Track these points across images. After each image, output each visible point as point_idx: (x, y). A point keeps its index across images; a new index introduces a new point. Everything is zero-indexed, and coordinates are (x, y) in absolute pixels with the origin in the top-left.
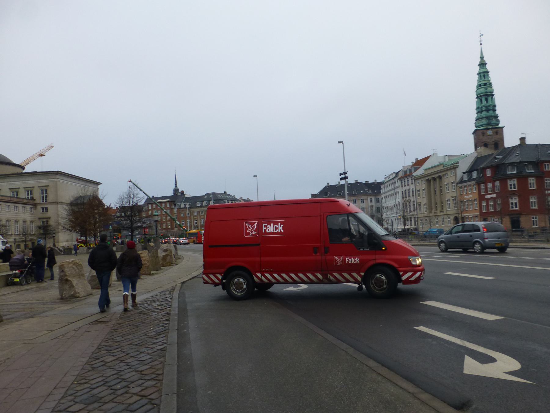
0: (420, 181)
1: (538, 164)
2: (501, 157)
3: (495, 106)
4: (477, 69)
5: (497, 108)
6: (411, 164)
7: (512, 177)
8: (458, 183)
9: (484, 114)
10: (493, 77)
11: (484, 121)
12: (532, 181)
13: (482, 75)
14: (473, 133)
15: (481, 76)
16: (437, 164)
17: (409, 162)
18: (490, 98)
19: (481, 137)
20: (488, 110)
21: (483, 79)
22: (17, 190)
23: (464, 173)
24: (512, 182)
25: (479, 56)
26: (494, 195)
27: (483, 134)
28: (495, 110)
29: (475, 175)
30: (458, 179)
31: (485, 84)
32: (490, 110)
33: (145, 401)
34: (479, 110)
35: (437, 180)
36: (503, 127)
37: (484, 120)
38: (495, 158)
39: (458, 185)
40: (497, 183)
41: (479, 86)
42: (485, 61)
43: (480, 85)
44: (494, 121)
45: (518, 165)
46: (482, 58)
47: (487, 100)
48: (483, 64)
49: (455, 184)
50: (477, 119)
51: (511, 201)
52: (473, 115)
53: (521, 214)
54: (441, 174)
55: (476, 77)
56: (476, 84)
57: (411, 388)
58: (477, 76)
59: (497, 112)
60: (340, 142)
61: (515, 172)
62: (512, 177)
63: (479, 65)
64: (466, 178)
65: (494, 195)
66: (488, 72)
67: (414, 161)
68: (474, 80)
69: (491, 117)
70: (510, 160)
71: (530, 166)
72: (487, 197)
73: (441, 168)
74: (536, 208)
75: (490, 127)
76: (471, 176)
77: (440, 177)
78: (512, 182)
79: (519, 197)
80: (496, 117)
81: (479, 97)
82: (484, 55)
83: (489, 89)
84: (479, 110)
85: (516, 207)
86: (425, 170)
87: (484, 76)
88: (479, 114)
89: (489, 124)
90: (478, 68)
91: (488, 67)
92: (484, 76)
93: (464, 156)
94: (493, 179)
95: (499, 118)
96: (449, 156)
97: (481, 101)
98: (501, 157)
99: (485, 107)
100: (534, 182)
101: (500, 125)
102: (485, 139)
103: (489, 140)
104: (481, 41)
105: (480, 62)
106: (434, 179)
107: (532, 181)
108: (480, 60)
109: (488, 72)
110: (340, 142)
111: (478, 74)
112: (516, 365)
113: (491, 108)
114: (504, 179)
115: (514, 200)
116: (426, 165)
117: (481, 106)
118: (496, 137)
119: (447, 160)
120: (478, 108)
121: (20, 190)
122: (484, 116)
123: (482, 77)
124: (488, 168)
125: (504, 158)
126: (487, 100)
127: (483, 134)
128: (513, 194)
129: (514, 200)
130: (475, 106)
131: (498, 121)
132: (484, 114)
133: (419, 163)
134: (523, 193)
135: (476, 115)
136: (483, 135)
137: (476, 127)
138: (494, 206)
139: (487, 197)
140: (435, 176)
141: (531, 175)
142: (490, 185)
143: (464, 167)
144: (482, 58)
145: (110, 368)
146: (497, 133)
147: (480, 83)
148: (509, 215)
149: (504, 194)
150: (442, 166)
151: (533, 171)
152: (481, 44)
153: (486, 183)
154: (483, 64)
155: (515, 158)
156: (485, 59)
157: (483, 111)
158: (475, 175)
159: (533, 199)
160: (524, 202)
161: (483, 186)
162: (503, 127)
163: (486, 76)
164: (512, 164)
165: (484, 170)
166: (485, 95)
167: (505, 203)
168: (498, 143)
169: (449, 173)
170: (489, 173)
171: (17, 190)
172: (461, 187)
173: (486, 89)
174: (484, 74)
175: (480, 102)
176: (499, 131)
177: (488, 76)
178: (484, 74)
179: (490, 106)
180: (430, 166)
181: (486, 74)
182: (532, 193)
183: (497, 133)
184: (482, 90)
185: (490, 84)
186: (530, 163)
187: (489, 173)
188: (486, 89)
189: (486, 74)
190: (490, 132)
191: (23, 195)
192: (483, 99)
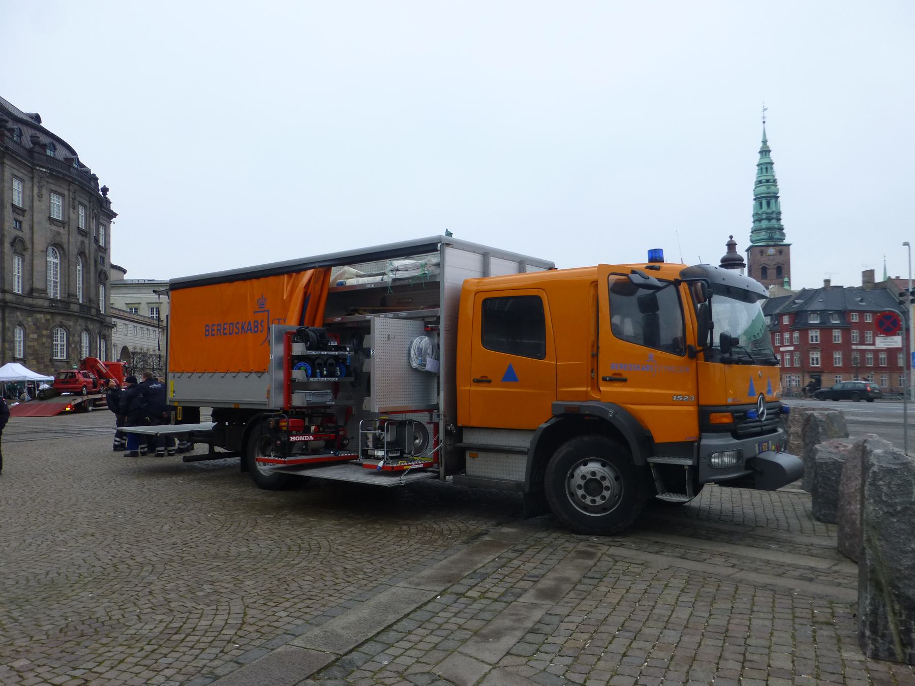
1: (844, 314)
3: (780, 213)
4: (757, 158)
5: (782, 216)
7: (814, 327)
9: (764, 224)
10: (779, 172)
11: (764, 235)
12: (837, 333)
13: (764, 167)
14: (747, 251)
15: (762, 169)
18: (773, 201)
19: (759, 256)
20: (769, 219)
21: (764, 173)
22: (136, 306)
24: (814, 334)
25: (761, 139)
26: (792, 348)
27: (762, 252)
28: (779, 220)
31: (768, 181)
34: (756, 218)
38: (795, 303)
40: (796, 334)
44: (777, 236)
45: (823, 313)
46: (765, 142)
47: (768, 204)
48: (765, 152)
50: (754, 231)
51: (811, 356)
53: (823, 372)
55: (755, 170)
59: (782, 222)
61: (818, 322)
62: (814, 327)
65: (792, 348)
66: (773, 164)
68: (752, 174)
69: (774, 228)
70: (812, 307)
71: (836, 316)
72: (782, 349)
78: (814, 334)
79: (822, 351)
80: (781, 229)
81: (758, 199)
82: (768, 138)
83: (773, 187)
84: (758, 218)
87: (767, 168)
88: (757, 224)
89: (771, 238)
90: (759, 156)
91: (773, 156)
92: (767, 168)
94: (791, 329)
97: (761, 204)
99: (766, 213)
101: (786, 242)
102: (763, 260)
103: (769, 263)
104: (764, 118)
105: (762, 148)
107: (837, 333)
108: (761, 145)
109: (773, 164)
113: (774, 216)
114: (805, 330)
115: (816, 355)
117: (760, 212)
118: (780, 259)
120: (755, 215)
121: (141, 306)
122: (764, 227)
123: (764, 170)
125: (806, 303)
126: (768, 204)
127: (762, 252)
128: (814, 347)
129: (816, 355)
130: (751, 212)
131: (784, 235)
132: (764, 224)
134: (827, 348)
135: (752, 225)
137: (752, 241)
138: (792, 360)
139: (782, 349)
141: (836, 327)
142: (787, 335)
144: (765, 142)
146: (781, 252)
148: (809, 372)
149: (804, 348)
151: (838, 322)
153: (781, 332)
154: (765, 152)
155: (818, 305)
156: (768, 144)
157: (762, 219)
159: (837, 355)
160: (827, 358)
161: (777, 337)
164: (814, 312)
165: (780, 316)
167: (805, 359)
170: (786, 320)
171: (136, 306)
173: (769, 188)
174: (766, 167)
176: (784, 250)
177: (772, 168)
178: (766, 167)
179: (773, 213)
181: (769, 166)
182: (837, 347)
183: (781, 252)
184: (763, 189)
185: (775, 181)
186: (837, 312)
187: (786, 320)
188: (769, 188)
189: (769, 166)
190: (771, 251)
191: (145, 312)
192: (764, 202)
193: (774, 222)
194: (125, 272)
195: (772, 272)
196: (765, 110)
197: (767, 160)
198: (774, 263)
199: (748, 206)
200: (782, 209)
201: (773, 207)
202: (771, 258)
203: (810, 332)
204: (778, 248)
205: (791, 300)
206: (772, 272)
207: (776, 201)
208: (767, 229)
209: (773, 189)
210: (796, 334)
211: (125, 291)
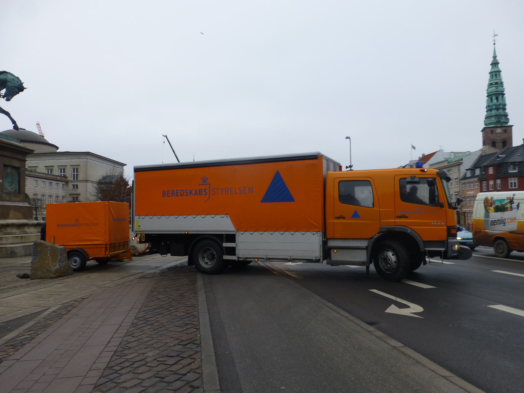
2: (504, 156)
3: (505, 105)
4: (489, 68)
5: (507, 107)
6: (418, 159)
7: (513, 175)
9: (494, 112)
10: (505, 77)
11: (493, 120)
13: (494, 74)
14: (482, 131)
15: (492, 75)
16: (443, 159)
17: (416, 156)
18: (500, 97)
20: (497, 109)
22: (51, 168)
23: (467, 170)
25: (492, 55)
27: (492, 132)
28: (504, 109)
29: (478, 172)
30: (462, 175)
31: (497, 83)
33: (188, 315)
34: (488, 108)
36: (512, 126)
37: (493, 119)
38: (498, 157)
39: (461, 181)
40: (499, 181)
41: (491, 85)
42: (497, 60)
43: (491, 84)
44: (503, 120)
46: (495, 57)
47: (497, 99)
48: (495, 64)
50: (486, 118)
52: (483, 113)
55: (488, 76)
56: (487, 83)
57: (346, 314)
58: (489, 75)
59: (507, 111)
60: (347, 138)
61: (516, 171)
62: (513, 175)
63: (491, 64)
64: (469, 174)
66: (500, 72)
67: (421, 156)
68: (486, 79)
69: (501, 115)
73: (446, 164)
75: (499, 125)
76: (474, 173)
80: (506, 115)
81: (490, 96)
82: (497, 54)
83: (500, 87)
84: (489, 109)
86: (431, 165)
87: (496, 75)
89: (498, 122)
90: (490, 67)
91: (501, 67)
92: (496, 75)
93: (469, 154)
94: (494, 177)
95: (508, 117)
96: (455, 153)
97: (492, 99)
98: (504, 156)
99: (495, 105)
101: (509, 124)
102: (493, 137)
103: (497, 138)
104: (494, 41)
108: (492, 59)
109: (500, 72)
110: (347, 138)
111: (490, 73)
112: (420, 309)
113: (501, 106)
116: (432, 161)
117: (491, 104)
118: (505, 136)
119: (452, 157)
120: (488, 106)
121: (54, 168)
122: (493, 114)
123: (494, 76)
124: (490, 166)
127: (492, 132)
130: (485, 105)
131: (508, 119)
132: (494, 112)
133: (426, 158)
135: (486, 113)
137: (485, 125)
142: (491, 183)
143: (468, 164)
144: (495, 57)
145: (163, 301)
146: (505, 131)
150: (447, 162)
152: (494, 44)
153: (487, 180)
154: (495, 64)
155: (517, 158)
156: (497, 58)
162: (512, 126)
163: (498, 76)
164: (514, 164)
165: (486, 168)
166: (496, 95)
168: (507, 141)
169: (453, 169)
170: (491, 171)
171: (51, 168)
172: (464, 184)
173: (497, 88)
174: (495, 73)
175: (490, 101)
176: (508, 130)
177: (500, 75)
178: (495, 73)
179: (500, 105)
180: (436, 162)
181: (497, 73)
183: (505, 131)
184: (493, 89)
185: (502, 83)
187: (491, 171)
188: (497, 88)
189: (497, 73)
190: (499, 130)
191: (56, 172)
192: (494, 98)
193: (501, 111)
194: (57, 148)
196: (495, 35)
197: (496, 69)
198: (501, 138)
201: (500, 101)
202: (498, 135)
203: (509, 179)
205: (496, 155)
208: (496, 116)
209: (500, 89)
210: (499, 181)
211: (44, 158)
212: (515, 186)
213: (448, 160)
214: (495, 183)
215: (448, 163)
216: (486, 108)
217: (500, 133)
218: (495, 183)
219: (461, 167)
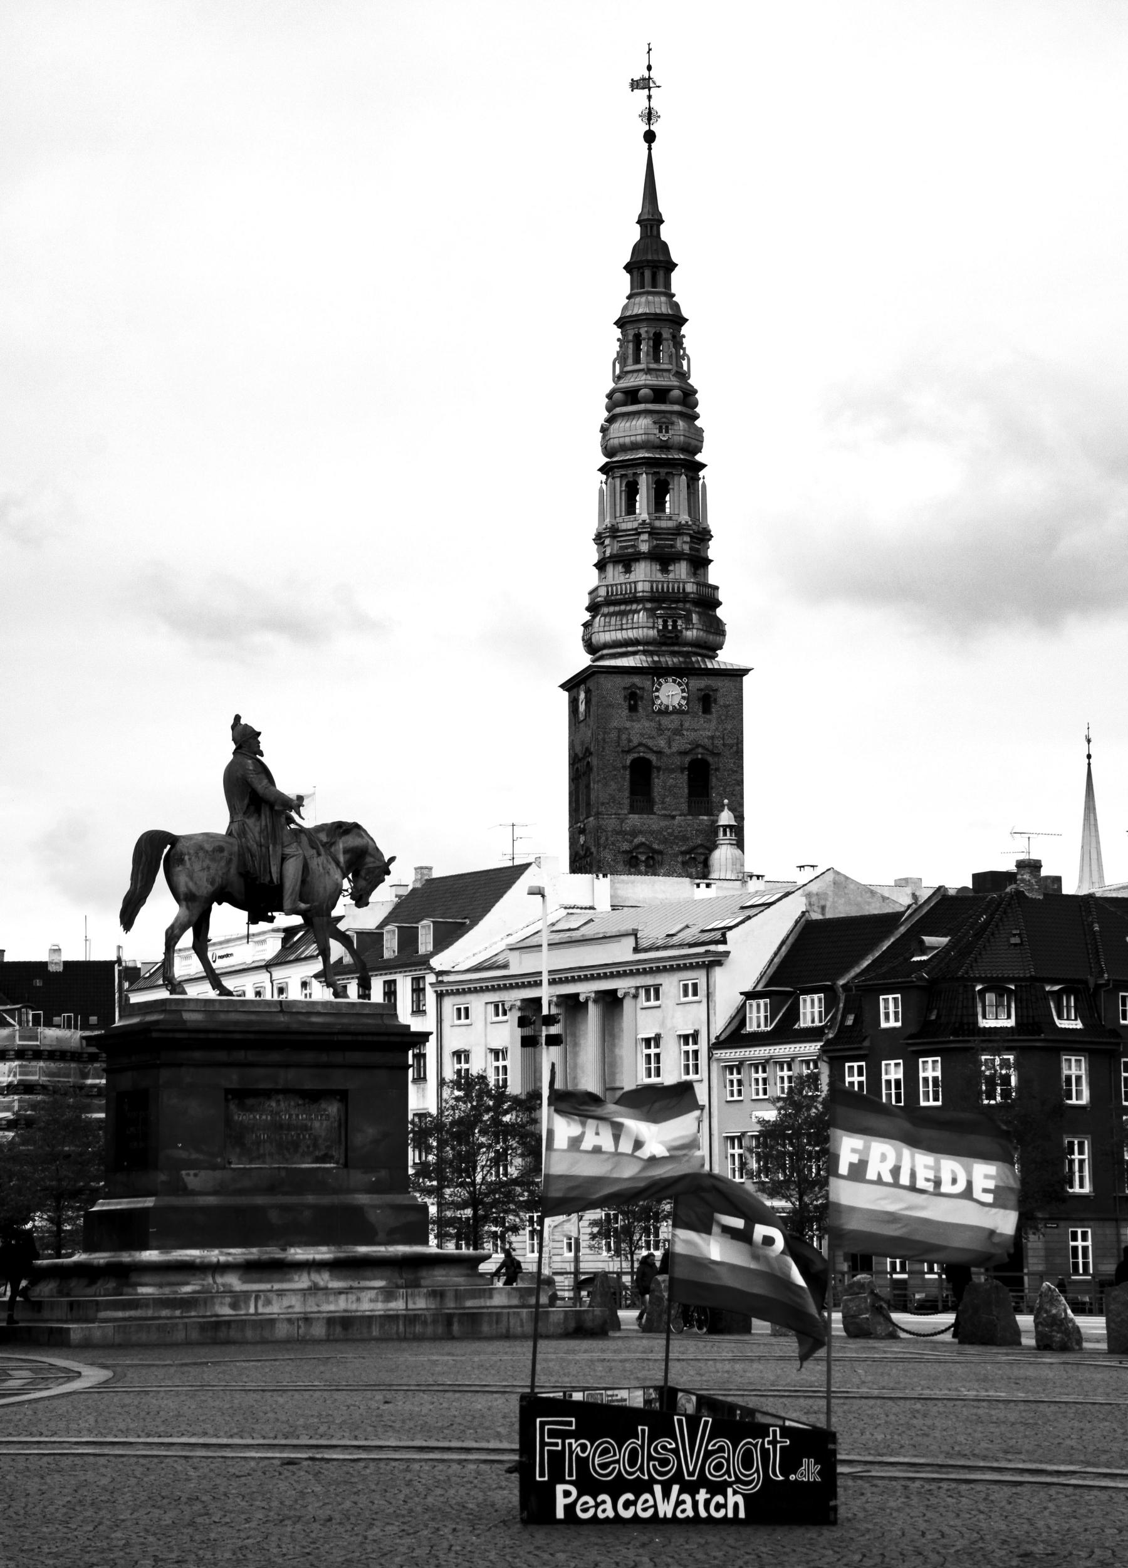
0: (478, 1004)
3: (703, 536)
7: (996, 1040)
8: (720, 1044)
9: (643, 576)
11: (640, 625)
12: (1075, 1068)
19: (620, 717)
20: (663, 559)
23: (749, 995)
24: (998, 1064)
27: (635, 700)
28: (700, 563)
30: (720, 1024)
31: (660, 395)
32: (677, 557)
35: (593, 1011)
36: (746, 671)
39: (720, 1054)
40: (930, 1069)
42: (665, 247)
46: (651, 221)
48: (651, 264)
49: (703, 1046)
54: (622, 985)
56: (603, 381)
58: (617, 333)
59: (714, 575)
61: (1011, 1023)
64: (757, 1019)
66: (683, 321)
69: (684, 598)
73: (622, 952)
74: (1087, 1189)
76: (794, 1014)
77: (611, 1002)
80: (708, 601)
81: (619, 466)
82: (664, 206)
84: (615, 551)
85: (1082, 1186)
87: (657, 340)
88: (615, 575)
89: (668, 640)
90: (624, 282)
92: (657, 340)
94: (909, 1046)
95: (720, 612)
97: (632, 491)
99: (654, 533)
100: (1083, 1072)
101: (726, 657)
106: (573, 1005)
108: (634, 234)
109: (683, 321)
111: (621, 323)
113: (683, 544)
117: (628, 524)
118: (703, 730)
130: (592, 526)
131: (717, 628)
132: (643, 576)
135: (592, 578)
136: (633, 709)
137: (591, 647)
140: (585, 989)
144: (651, 221)
147: (629, 382)
150: (630, 942)
151: (1078, 1025)
152: (650, 137)
154: (651, 264)
157: (638, 557)
158: (811, 1010)
163: (666, 348)
170: (890, 1013)
172: (739, 1067)
175: (621, 504)
177: (677, 341)
179: (679, 530)
183: (705, 701)
184: (637, 428)
185: (689, 396)
187: (890, 1013)
189: (666, 334)
190: (670, 694)
193: (681, 570)
195: (670, 786)
197: (659, 306)
199: (571, 500)
200: (714, 521)
202: (665, 721)
204: (697, 683)
206: (670, 786)
207: (693, 480)
208: (658, 600)
210: (930, 1069)
212: (851, 1068)
213: (634, 933)
214: (911, 1073)
215: (636, 950)
216: (599, 539)
217: (678, 711)
218: (911, 1073)
219: (718, 972)
